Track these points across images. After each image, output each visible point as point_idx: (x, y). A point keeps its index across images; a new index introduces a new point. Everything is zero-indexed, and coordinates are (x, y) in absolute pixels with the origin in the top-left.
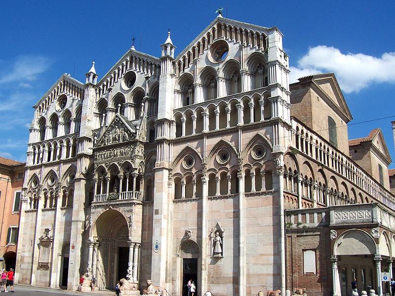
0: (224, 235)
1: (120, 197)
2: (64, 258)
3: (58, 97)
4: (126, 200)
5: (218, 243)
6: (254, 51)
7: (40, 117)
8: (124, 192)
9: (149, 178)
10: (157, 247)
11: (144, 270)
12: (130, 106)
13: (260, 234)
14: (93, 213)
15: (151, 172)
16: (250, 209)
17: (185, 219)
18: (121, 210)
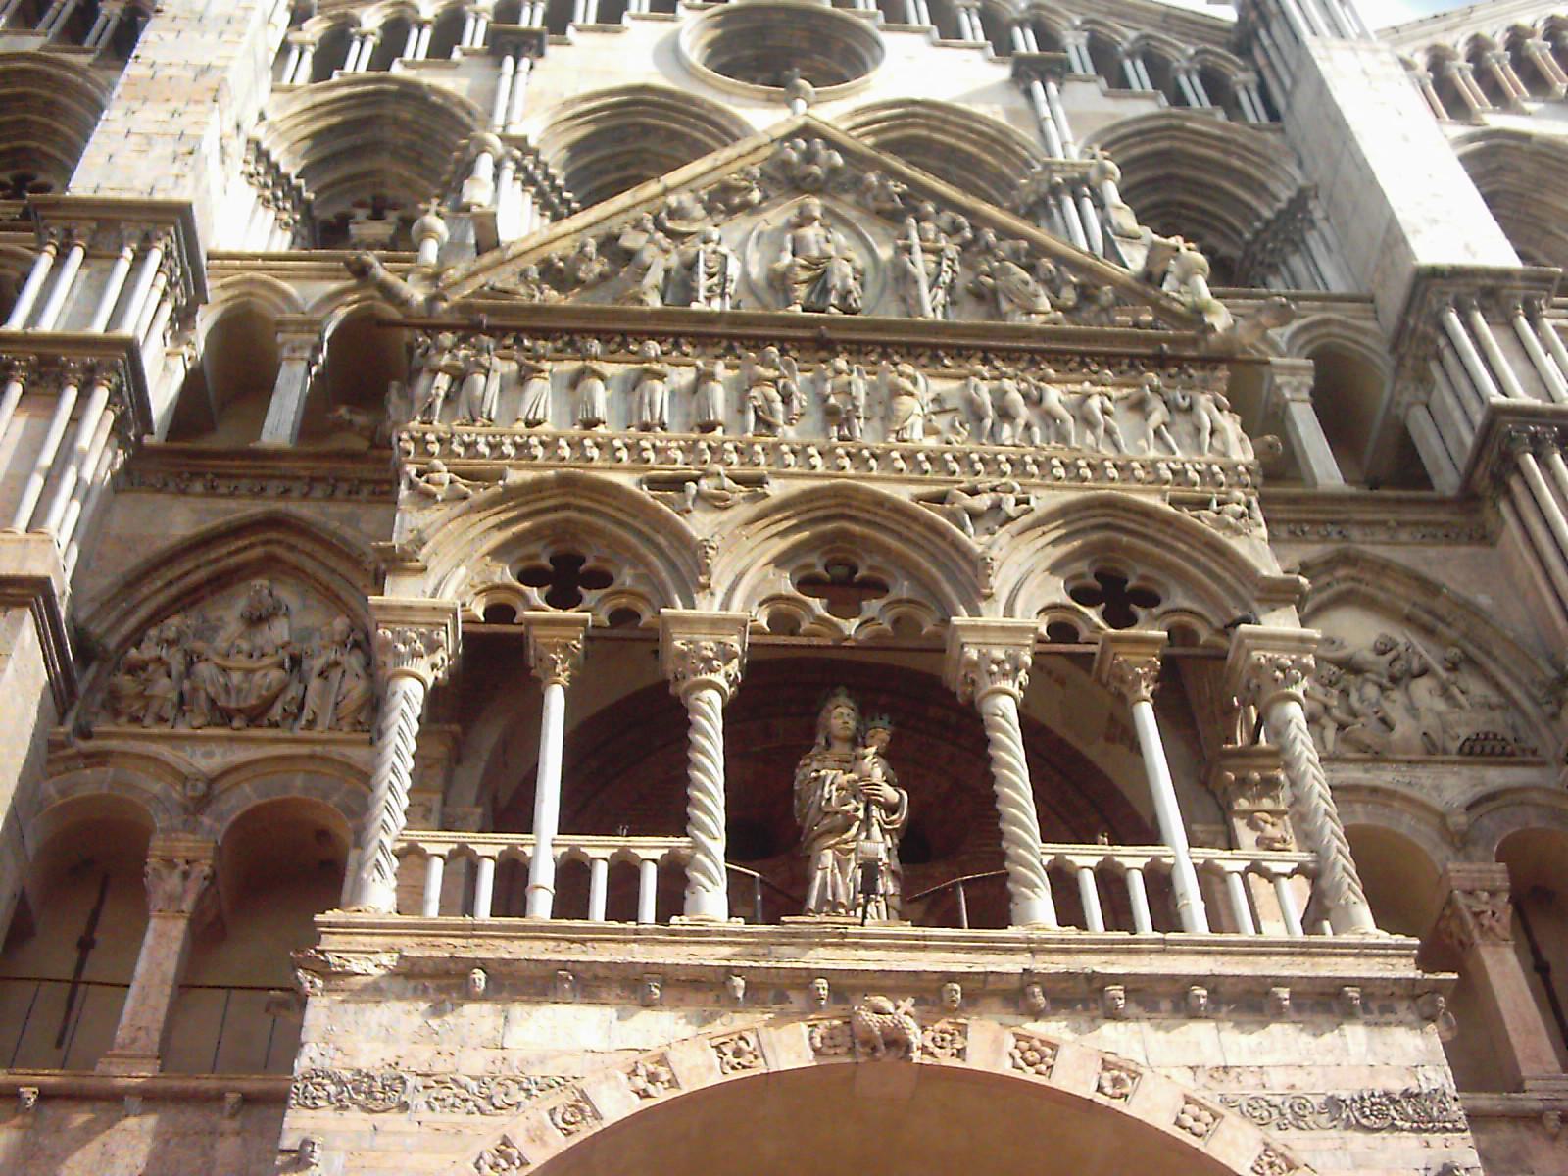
8: (1133, 859)
15: (1376, 756)
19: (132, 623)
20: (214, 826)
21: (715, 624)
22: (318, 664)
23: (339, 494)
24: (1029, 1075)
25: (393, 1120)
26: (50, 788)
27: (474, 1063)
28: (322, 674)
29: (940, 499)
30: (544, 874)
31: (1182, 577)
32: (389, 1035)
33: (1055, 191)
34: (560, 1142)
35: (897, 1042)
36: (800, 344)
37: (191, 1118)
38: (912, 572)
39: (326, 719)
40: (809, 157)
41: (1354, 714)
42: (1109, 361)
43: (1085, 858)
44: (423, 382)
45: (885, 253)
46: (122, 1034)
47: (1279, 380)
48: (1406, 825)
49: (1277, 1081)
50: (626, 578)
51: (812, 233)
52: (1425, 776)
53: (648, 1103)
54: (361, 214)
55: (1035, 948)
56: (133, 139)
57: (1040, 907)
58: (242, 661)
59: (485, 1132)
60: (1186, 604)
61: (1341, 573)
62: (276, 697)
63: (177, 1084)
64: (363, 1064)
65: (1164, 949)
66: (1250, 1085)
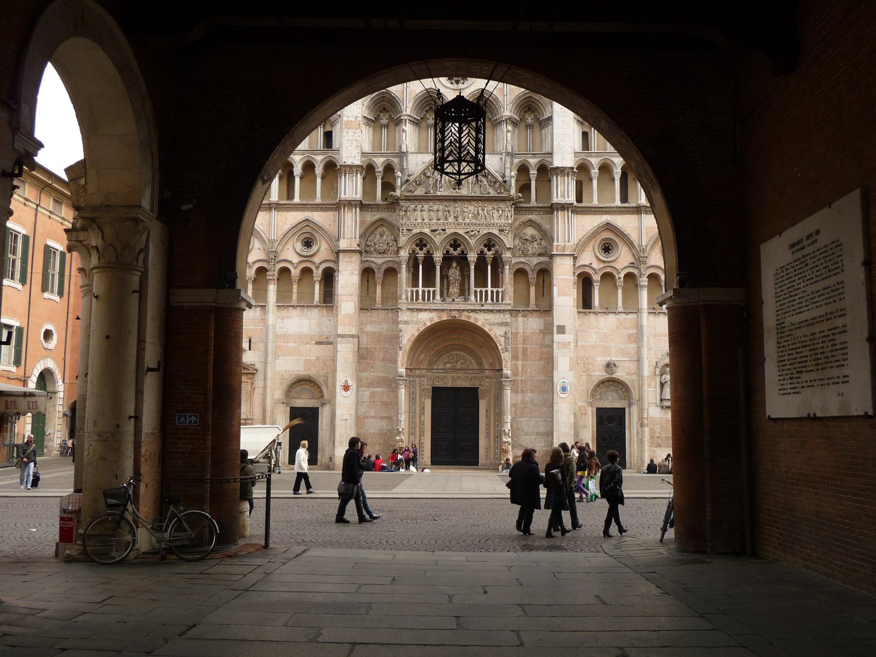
1: (473, 297)
2: (290, 407)
4: (488, 304)
8: (484, 290)
9: (521, 266)
10: (564, 389)
11: (518, 429)
14: (407, 323)
15: (526, 256)
17: (603, 343)
18: (480, 320)
19: (366, 238)
20: (382, 271)
21: (439, 257)
22: (391, 245)
23: (389, 210)
24: (468, 320)
25: (408, 326)
28: (391, 246)
29: (468, 232)
30: (420, 293)
31: (498, 244)
32: (407, 317)
33: (503, 121)
34: (424, 328)
36: (452, 200)
37: (386, 311)
38: (464, 245)
39: (393, 253)
41: (525, 248)
42: (495, 200)
43: (478, 290)
44: (401, 212)
46: (377, 301)
47: (531, 176)
49: (492, 320)
50: (428, 246)
52: (531, 259)
53: (431, 324)
54: (381, 114)
55: (470, 304)
56: (349, 141)
57: (473, 297)
59: (417, 326)
60: (498, 248)
61: (529, 222)
62: (385, 251)
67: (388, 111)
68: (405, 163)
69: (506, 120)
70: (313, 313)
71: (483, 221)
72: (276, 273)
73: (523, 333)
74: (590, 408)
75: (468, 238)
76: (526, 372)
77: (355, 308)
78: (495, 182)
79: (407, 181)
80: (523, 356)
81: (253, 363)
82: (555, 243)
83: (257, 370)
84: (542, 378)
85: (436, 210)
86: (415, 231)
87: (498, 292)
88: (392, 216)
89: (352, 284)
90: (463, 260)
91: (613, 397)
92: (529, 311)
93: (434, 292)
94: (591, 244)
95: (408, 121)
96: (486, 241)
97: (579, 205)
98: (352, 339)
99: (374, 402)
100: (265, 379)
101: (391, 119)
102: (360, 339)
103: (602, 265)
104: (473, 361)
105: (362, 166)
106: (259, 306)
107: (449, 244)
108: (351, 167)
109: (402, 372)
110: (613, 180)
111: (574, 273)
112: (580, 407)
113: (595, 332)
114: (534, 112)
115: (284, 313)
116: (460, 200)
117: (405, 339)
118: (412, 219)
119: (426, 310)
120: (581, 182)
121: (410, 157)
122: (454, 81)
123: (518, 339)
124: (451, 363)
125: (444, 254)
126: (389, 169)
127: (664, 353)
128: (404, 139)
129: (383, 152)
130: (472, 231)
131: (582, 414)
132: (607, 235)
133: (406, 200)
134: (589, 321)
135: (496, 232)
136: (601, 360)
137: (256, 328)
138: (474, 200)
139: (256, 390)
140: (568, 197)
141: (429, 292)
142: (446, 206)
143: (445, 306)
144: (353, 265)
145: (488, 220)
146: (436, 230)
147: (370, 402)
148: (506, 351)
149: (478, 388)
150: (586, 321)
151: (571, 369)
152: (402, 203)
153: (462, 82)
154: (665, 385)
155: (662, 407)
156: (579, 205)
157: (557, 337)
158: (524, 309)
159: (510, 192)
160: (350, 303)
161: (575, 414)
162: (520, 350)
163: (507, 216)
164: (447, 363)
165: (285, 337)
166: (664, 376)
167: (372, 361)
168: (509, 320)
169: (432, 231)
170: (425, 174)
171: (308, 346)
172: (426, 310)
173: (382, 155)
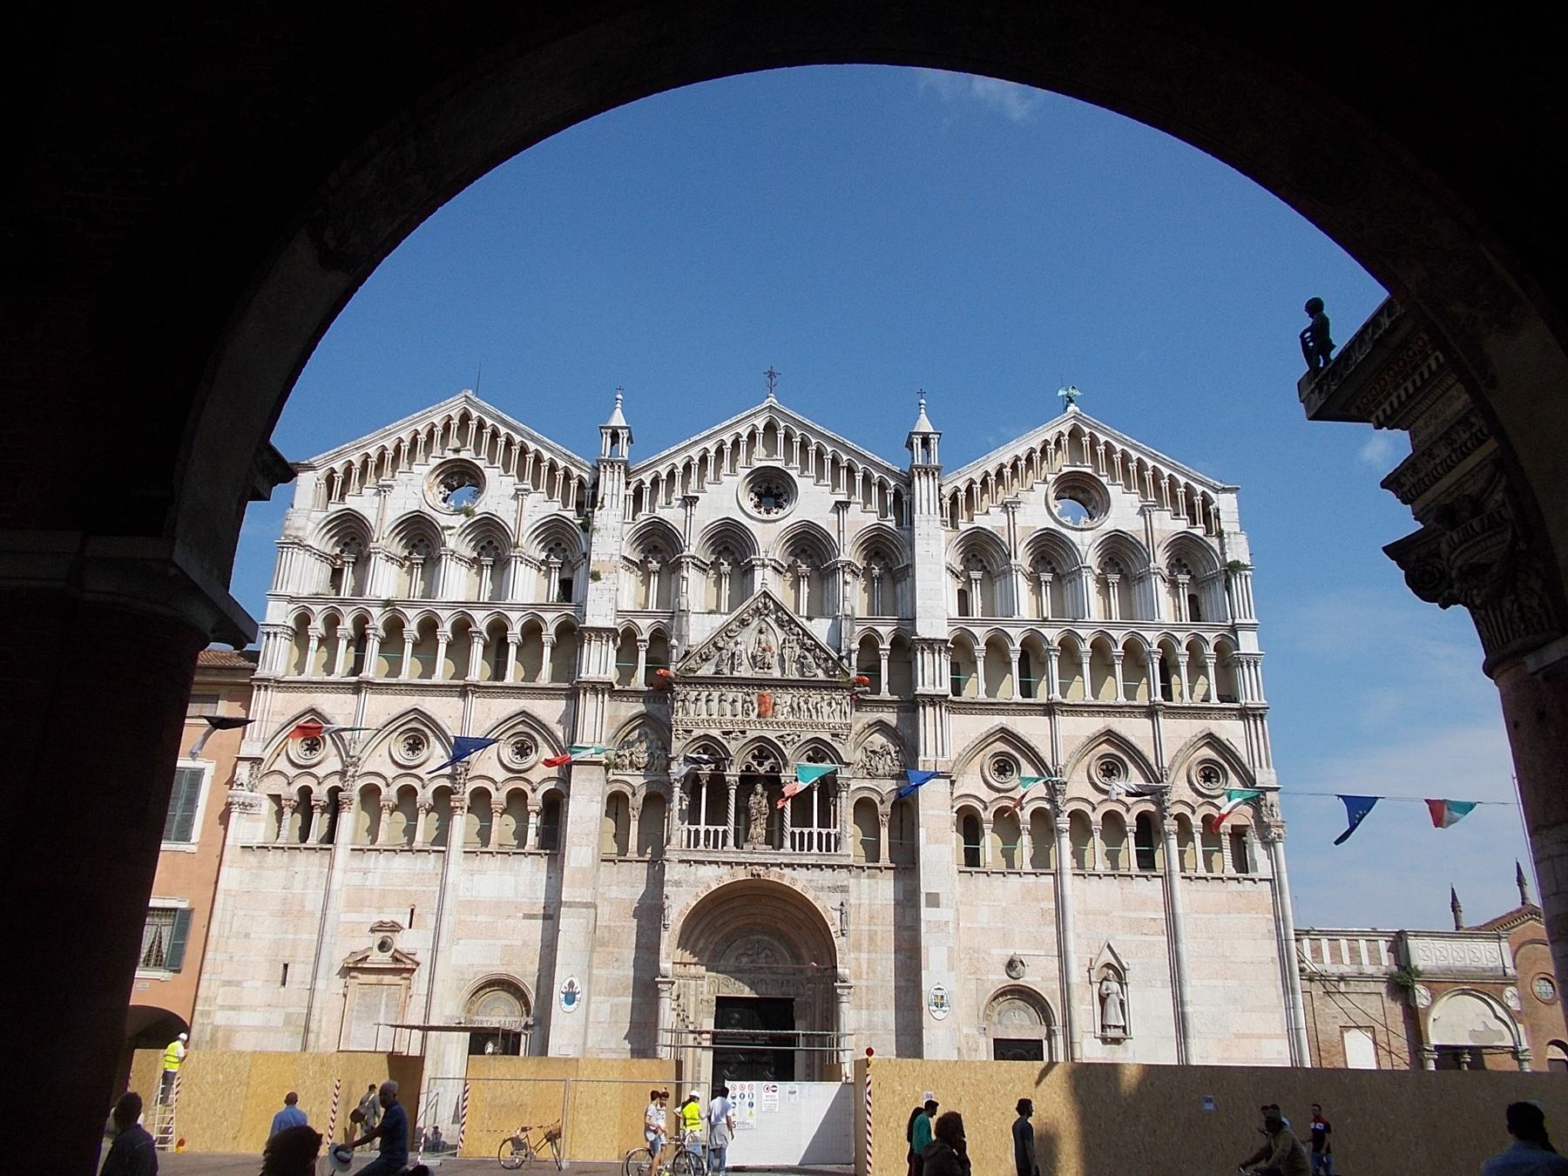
0: (1129, 977)
1: (787, 843)
3: (434, 462)
5: (1114, 996)
6: (1182, 525)
7: (335, 507)
8: (806, 831)
9: (866, 794)
12: (774, 568)
13: (1231, 983)
14: (678, 884)
15: (872, 776)
16: (1196, 915)
17: (1001, 925)
18: (800, 881)
21: (734, 776)
25: (680, 889)
26: (607, 788)
27: (692, 878)
29: (782, 736)
30: (702, 835)
35: (759, 875)
37: (646, 864)
38: (776, 759)
40: (765, 603)
43: (797, 830)
45: (781, 642)
48: (877, 799)
51: (762, 637)
57: (787, 843)
58: (642, 755)
59: (694, 890)
63: (641, 859)
64: (676, 878)
65: (807, 855)
66: (815, 884)
67: (661, 552)
68: (685, 628)
69: (843, 567)
70: (524, 864)
71: (805, 718)
72: (467, 796)
73: (870, 905)
74: (984, 1038)
75: (782, 746)
76: (874, 972)
77: (593, 857)
78: (826, 660)
79: (687, 653)
80: (870, 945)
81: (411, 951)
82: (921, 758)
83: (418, 964)
84: (902, 984)
85: (731, 700)
86: (696, 733)
87: (828, 835)
88: (659, 709)
89: (591, 818)
90: (773, 784)
91: (1021, 1020)
92: (880, 868)
93: (725, 832)
94: (978, 759)
95: (690, 564)
96: (810, 752)
97: (957, 699)
98: (584, 910)
99: (616, 1022)
100: (431, 980)
101: (663, 562)
102: (599, 911)
103: (997, 795)
104: (784, 951)
105: (616, 629)
106: (434, 851)
107: (750, 756)
108: (598, 631)
109: (666, 970)
110: (1009, 664)
111: (952, 807)
112: (967, 1036)
113: (988, 906)
114: (883, 559)
115: (476, 862)
116: (770, 686)
117: (674, 911)
118: (692, 713)
119: (710, 862)
120: (957, 664)
121: (692, 618)
122: (762, 510)
123: (861, 915)
124: (749, 955)
125: (742, 771)
126: (659, 638)
127: (1102, 945)
128: (684, 590)
129: (650, 609)
130: (789, 735)
131: (970, 1049)
132: (1000, 747)
133: (685, 684)
134: (976, 887)
135: (827, 737)
136: (1001, 955)
137: (425, 889)
138: (792, 687)
139: (413, 998)
140: (941, 685)
141: (716, 832)
142: (749, 695)
143: (742, 858)
144: (594, 784)
145: (814, 717)
146: (731, 733)
147: (609, 1023)
148: (843, 935)
149: (793, 1000)
150: (973, 887)
151: (951, 968)
152: (677, 688)
153: (775, 510)
154: (1109, 1000)
155: (1105, 1040)
156: (957, 699)
157: (926, 913)
158: (871, 865)
159: (849, 674)
160: (584, 849)
161: (959, 1049)
162: (865, 934)
163: (845, 713)
164: (742, 955)
165: (471, 906)
166: (1105, 983)
167: (616, 950)
168: (845, 883)
169: (724, 733)
170: (715, 644)
171: (511, 921)
172: (710, 862)
173: (649, 615)
